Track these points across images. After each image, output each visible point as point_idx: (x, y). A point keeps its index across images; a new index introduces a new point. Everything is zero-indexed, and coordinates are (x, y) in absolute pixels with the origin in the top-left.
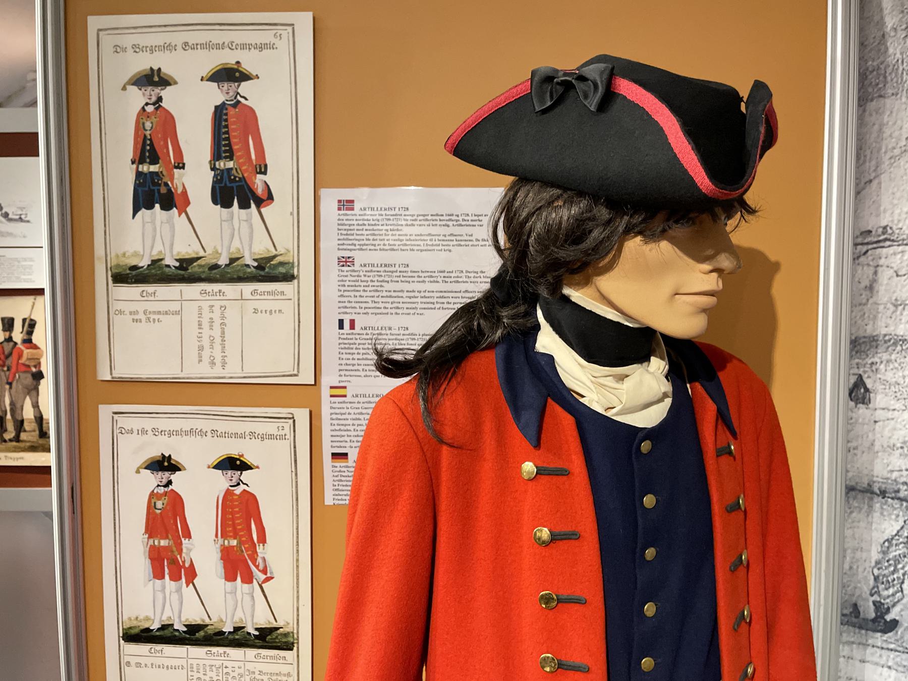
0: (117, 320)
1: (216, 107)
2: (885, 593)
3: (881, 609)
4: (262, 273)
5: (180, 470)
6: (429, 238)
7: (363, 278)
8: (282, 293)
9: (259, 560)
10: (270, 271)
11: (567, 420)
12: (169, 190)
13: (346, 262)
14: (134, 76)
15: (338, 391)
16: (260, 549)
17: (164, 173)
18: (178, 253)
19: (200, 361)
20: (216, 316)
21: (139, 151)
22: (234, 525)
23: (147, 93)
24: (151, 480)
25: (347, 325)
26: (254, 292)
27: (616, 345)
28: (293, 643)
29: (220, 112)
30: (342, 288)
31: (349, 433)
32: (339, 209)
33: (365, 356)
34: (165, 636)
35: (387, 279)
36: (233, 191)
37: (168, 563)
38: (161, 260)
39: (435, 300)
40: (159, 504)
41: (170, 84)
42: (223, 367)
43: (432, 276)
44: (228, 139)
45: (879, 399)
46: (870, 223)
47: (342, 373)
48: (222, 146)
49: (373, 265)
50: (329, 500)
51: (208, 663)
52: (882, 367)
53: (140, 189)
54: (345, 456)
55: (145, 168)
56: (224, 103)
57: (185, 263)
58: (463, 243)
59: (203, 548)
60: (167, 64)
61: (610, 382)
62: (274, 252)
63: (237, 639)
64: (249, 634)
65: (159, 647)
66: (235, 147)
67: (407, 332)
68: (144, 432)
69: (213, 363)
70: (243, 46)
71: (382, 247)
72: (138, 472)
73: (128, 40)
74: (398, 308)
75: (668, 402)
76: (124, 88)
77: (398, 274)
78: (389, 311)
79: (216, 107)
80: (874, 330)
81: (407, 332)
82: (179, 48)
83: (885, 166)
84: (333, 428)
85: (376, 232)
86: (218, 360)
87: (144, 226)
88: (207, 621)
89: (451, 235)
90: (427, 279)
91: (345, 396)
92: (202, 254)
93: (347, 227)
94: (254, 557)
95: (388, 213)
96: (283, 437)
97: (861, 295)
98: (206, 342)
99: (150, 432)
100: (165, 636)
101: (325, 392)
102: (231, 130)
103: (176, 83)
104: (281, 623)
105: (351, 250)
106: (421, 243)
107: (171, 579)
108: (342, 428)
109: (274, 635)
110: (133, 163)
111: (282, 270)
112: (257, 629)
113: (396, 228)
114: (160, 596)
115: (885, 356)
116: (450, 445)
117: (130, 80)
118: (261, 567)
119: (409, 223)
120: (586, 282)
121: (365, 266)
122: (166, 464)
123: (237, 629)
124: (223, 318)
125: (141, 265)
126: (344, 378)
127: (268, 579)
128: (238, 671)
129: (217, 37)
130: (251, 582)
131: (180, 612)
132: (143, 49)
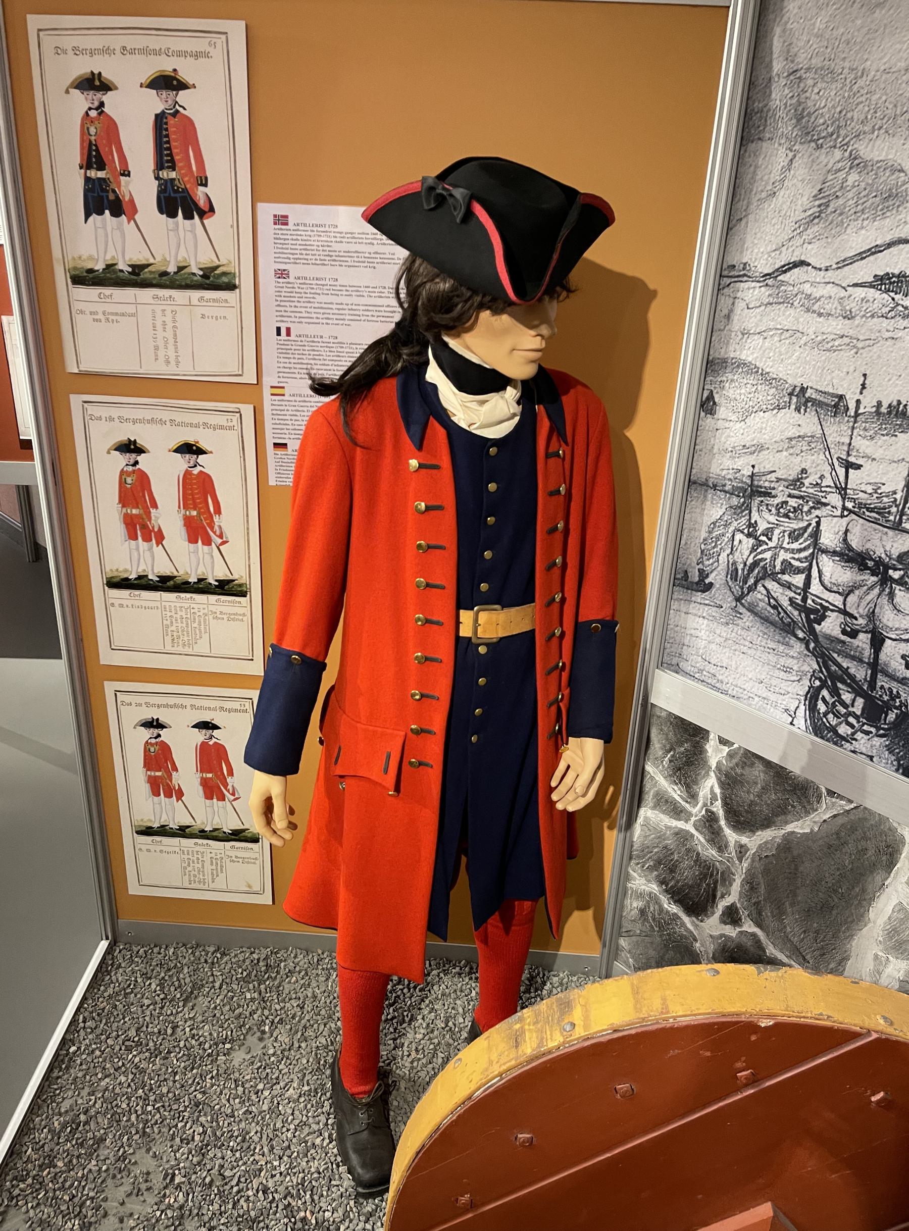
0: (78, 318)
1: (157, 116)
2: (707, 563)
3: (703, 574)
4: (208, 282)
5: (144, 452)
6: (355, 255)
7: (297, 290)
8: (226, 301)
9: (216, 528)
10: (214, 280)
11: (441, 432)
12: (117, 197)
13: (282, 274)
14: (76, 79)
15: (278, 390)
16: (216, 519)
17: (112, 180)
18: (130, 260)
19: (156, 359)
20: (169, 319)
21: (85, 157)
22: (194, 499)
23: (90, 97)
24: (121, 460)
25: (283, 332)
26: (201, 299)
27: (478, 380)
28: (246, 592)
29: (160, 120)
30: (279, 299)
31: (288, 427)
32: (275, 224)
33: (300, 361)
34: (141, 584)
35: (318, 291)
36: (177, 201)
37: (140, 527)
38: (115, 264)
39: (361, 313)
40: (129, 480)
41: (110, 89)
42: (177, 363)
43: (357, 291)
44: (169, 149)
45: (721, 412)
46: (734, 258)
47: (281, 375)
48: (164, 157)
49: (306, 278)
50: (272, 482)
51: (178, 605)
52: (727, 385)
53: (90, 194)
54: (284, 446)
55: (92, 174)
56: (163, 112)
57: (137, 269)
58: (386, 261)
59: (168, 515)
60: (108, 69)
61: (474, 405)
62: (218, 263)
63: (201, 587)
64: (210, 584)
65: (137, 592)
66: (177, 158)
67: (336, 341)
68: (111, 419)
69: (168, 362)
70: (180, 54)
71: (314, 262)
72: (109, 452)
73: (68, 42)
74: (328, 319)
75: (517, 419)
76: (67, 92)
77: (328, 287)
78: (321, 321)
79: (157, 116)
80: (726, 353)
81: (336, 341)
82: (118, 52)
83: (753, 207)
84: (274, 422)
85: (309, 247)
86: (172, 360)
87: (96, 230)
88: (176, 574)
89: (376, 253)
90: (354, 293)
91: (283, 395)
92: (152, 261)
93: (282, 241)
94: (211, 525)
95: (319, 229)
96: (231, 428)
97: (717, 323)
98: (160, 343)
99: (116, 420)
100: (141, 584)
101: (267, 392)
102: (171, 138)
103: (116, 88)
104: (235, 577)
105: (286, 263)
106: (349, 259)
107: (144, 540)
108: (282, 422)
109: (231, 585)
110: (81, 168)
111: (225, 279)
112: (216, 581)
113: (326, 244)
114: (135, 554)
115: (730, 376)
116: (361, 447)
117: (73, 82)
118: (218, 533)
119: (338, 240)
120: (457, 336)
121: (299, 278)
122: (132, 447)
123: (200, 580)
124: (174, 321)
125: (96, 268)
126: (281, 380)
127: (224, 543)
128: (203, 611)
129: (154, 42)
130: (210, 544)
131: (153, 566)
132: (83, 52)
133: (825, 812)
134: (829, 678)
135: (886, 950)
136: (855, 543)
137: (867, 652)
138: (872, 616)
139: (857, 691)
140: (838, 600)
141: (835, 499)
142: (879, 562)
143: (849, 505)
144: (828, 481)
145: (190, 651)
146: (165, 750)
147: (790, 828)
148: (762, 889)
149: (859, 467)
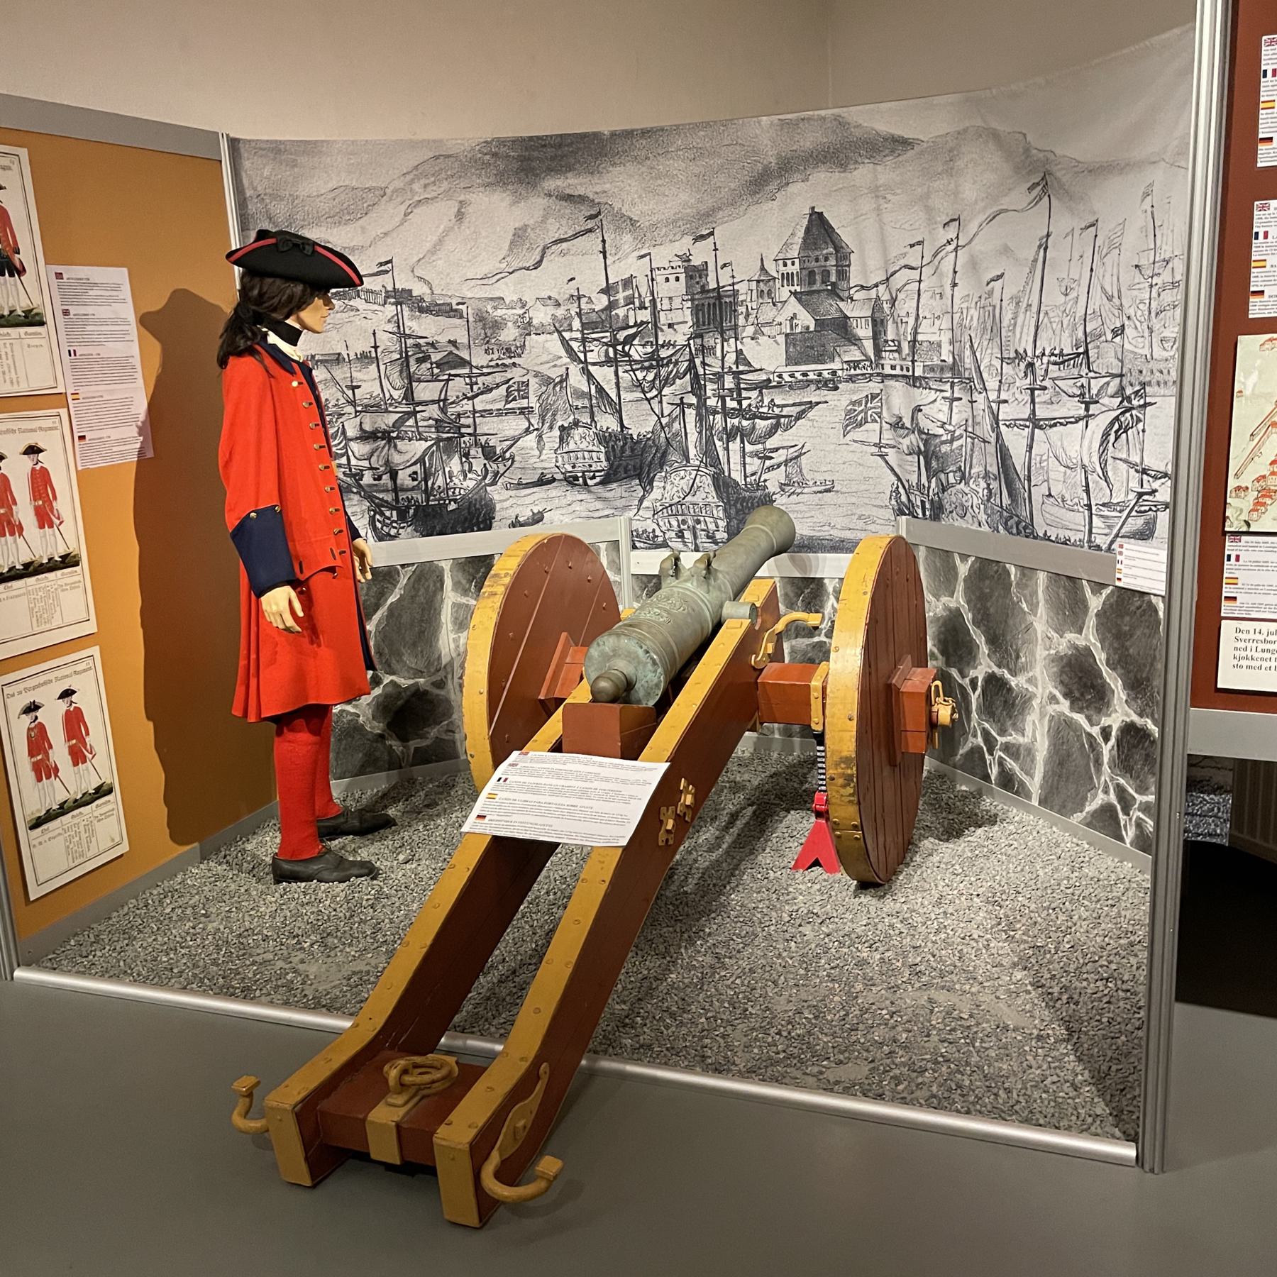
13: (66, 313)
65: (9, 584)
96: (56, 428)
111: (37, 318)
133: (403, 581)
134: (378, 507)
135: (457, 632)
136: (367, 427)
137: (390, 484)
138: (387, 463)
139: (391, 509)
140: (366, 463)
141: (350, 409)
142: (385, 432)
143: (359, 408)
144: (342, 401)
145: (48, 627)
146: (41, 729)
147: (389, 602)
148: (386, 651)
149: (359, 387)
